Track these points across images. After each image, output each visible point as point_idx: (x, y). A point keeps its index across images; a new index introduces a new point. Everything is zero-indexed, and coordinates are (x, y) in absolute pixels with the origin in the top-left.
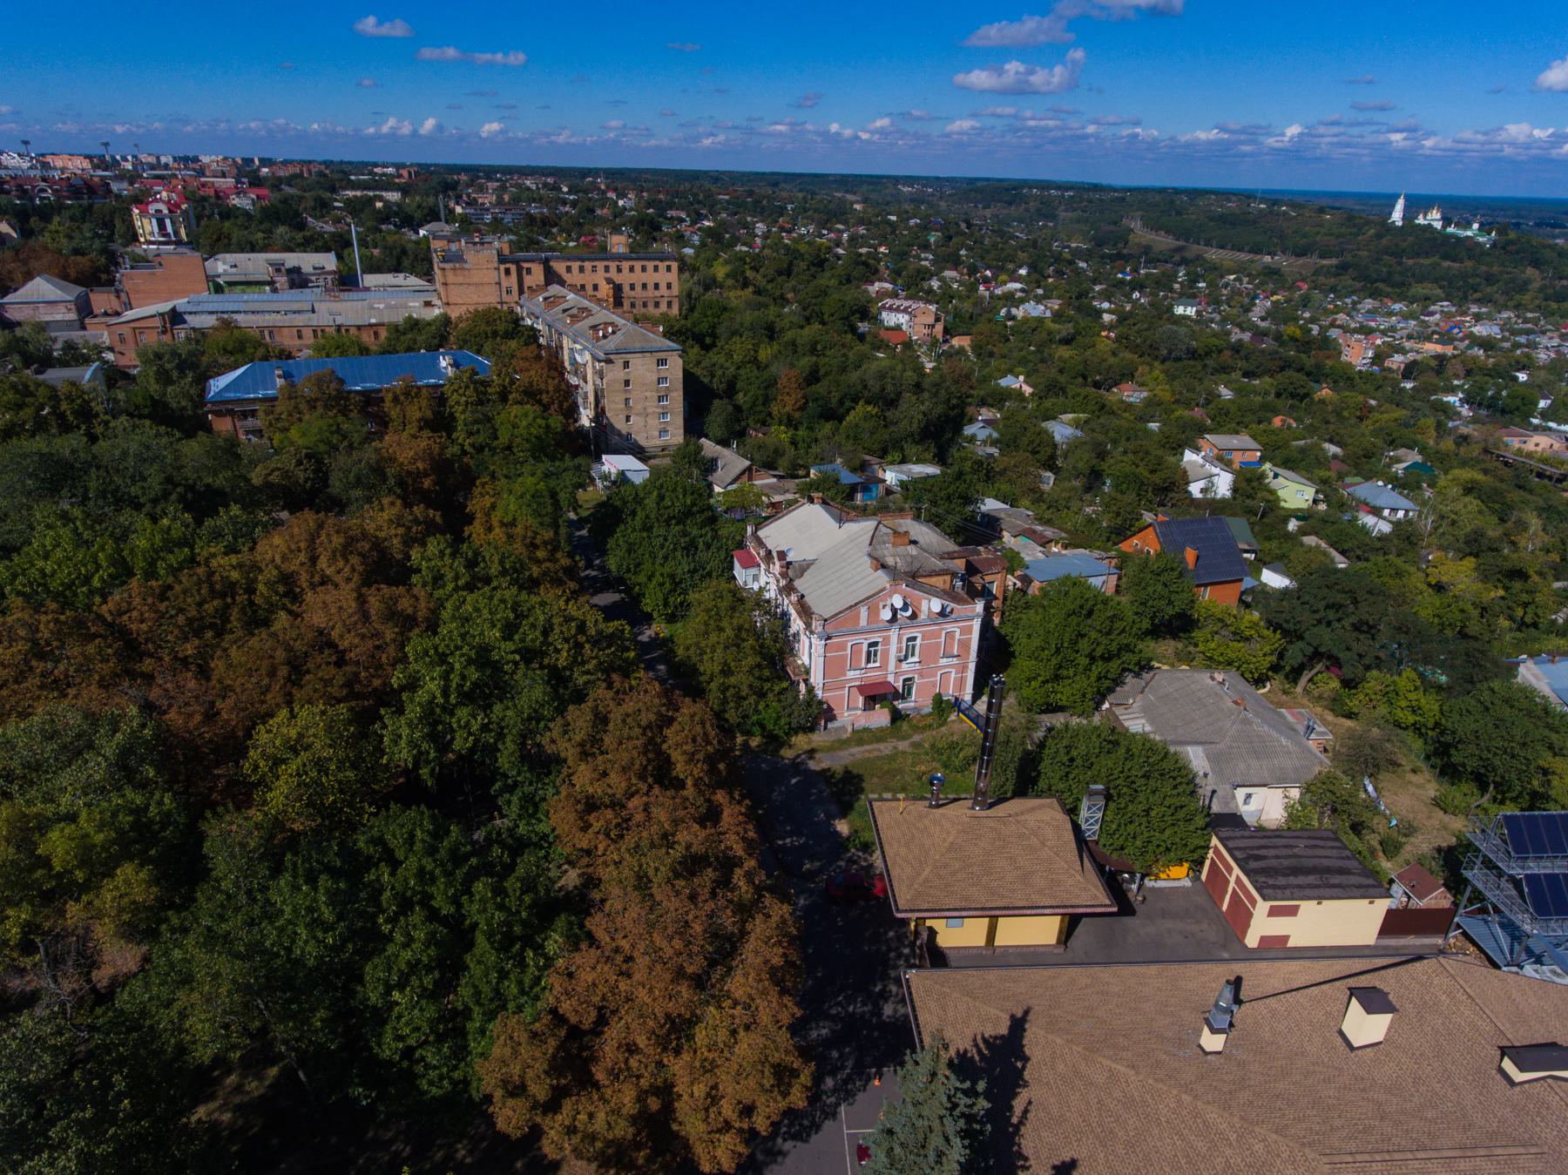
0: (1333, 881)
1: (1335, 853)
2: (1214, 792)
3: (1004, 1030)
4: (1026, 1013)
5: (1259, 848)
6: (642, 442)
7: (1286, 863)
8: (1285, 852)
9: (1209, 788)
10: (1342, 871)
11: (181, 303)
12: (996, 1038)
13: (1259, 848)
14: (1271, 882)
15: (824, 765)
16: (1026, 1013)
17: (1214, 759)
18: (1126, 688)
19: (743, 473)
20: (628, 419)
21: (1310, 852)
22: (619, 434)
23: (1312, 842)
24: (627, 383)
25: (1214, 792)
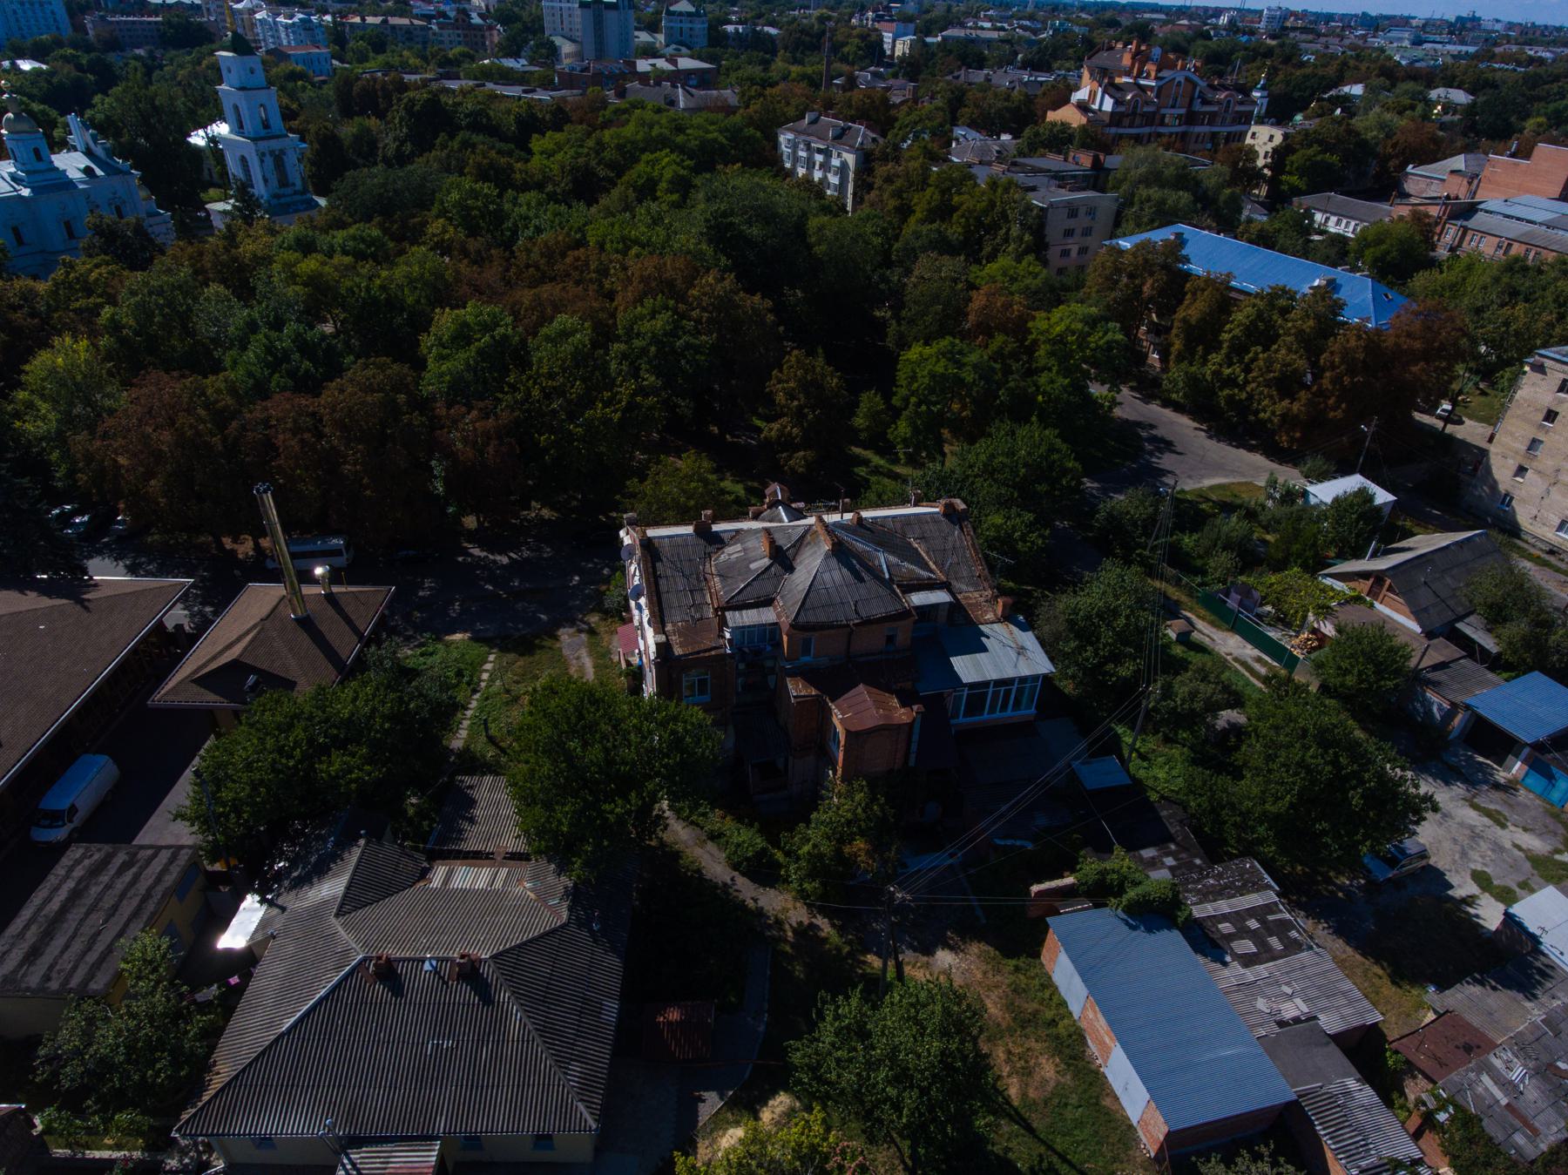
0: (34, 928)
1: (66, 964)
2: (283, 909)
4: (86, 608)
5: (136, 879)
6: (1523, 517)
7: (94, 891)
8: (108, 902)
9: (290, 906)
10: (33, 954)
11: (1493, 204)
13: (136, 879)
14: (87, 862)
16: (86, 608)
17: (318, 911)
18: (551, 879)
19: (1365, 575)
20: (1521, 470)
21: (87, 930)
22: (1494, 485)
23: (100, 947)
24: (1551, 416)
25: (283, 909)
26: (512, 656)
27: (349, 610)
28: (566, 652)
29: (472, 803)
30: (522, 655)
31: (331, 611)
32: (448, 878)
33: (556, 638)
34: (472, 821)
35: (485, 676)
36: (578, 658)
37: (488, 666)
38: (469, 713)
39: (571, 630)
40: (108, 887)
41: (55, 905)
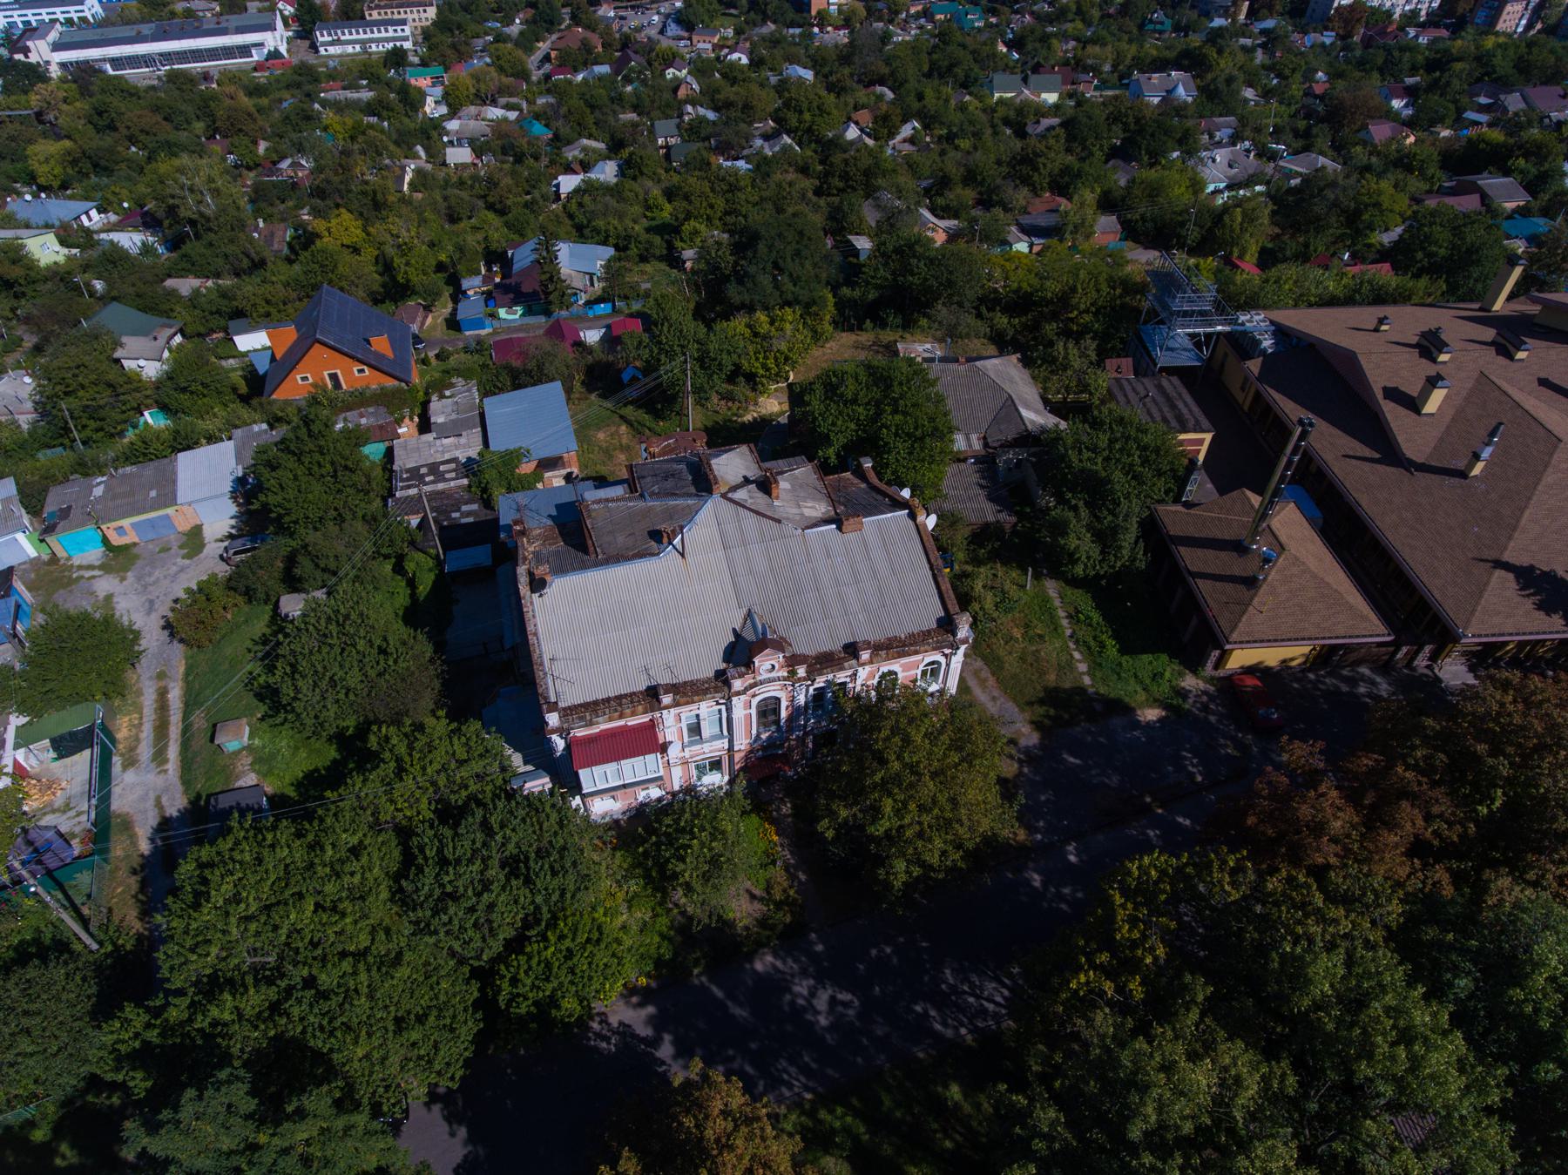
3: (1511, 576)
12: (1518, 583)
15: (1026, 729)
26: (1067, 685)
27: (1229, 587)
28: (1011, 708)
29: (991, 498)
30: (1056, 689)
31: (1237, 571)
32: (968, 439)
33: (1037, 725)
34: (982, 487)
35: (1077, 655)
36: (994, 699)
37: (1083, 667)
38: (1062, 614)
39: (1023, 742)
40: (1160, 410)
41: (1181, 405)
